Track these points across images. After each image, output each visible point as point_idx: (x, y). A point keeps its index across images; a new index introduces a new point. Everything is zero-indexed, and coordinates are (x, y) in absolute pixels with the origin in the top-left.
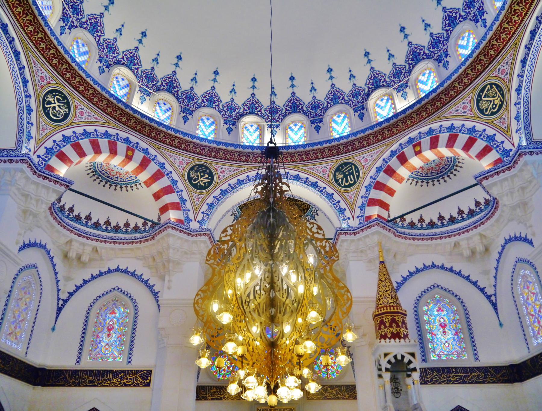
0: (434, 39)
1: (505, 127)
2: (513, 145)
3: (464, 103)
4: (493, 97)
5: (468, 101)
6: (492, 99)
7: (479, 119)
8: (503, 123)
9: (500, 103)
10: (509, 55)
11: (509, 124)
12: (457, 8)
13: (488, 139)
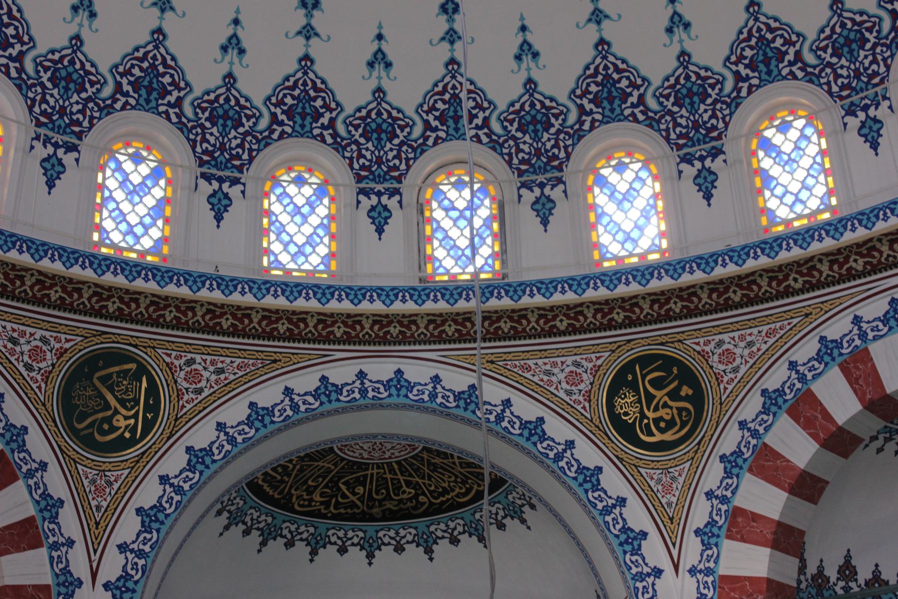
0: (72, 62)
1: (98, 508)
2: (94, 575)
3: (44, 340)
4: (122, 402)
5: (57, 346)
6: (113, 402)
7: (51, 423)
8: (100, 491)
9: (127, 435)
10: (238, 361)
11: (115, 511)
12: (188, 78)
13: (43, 504)
